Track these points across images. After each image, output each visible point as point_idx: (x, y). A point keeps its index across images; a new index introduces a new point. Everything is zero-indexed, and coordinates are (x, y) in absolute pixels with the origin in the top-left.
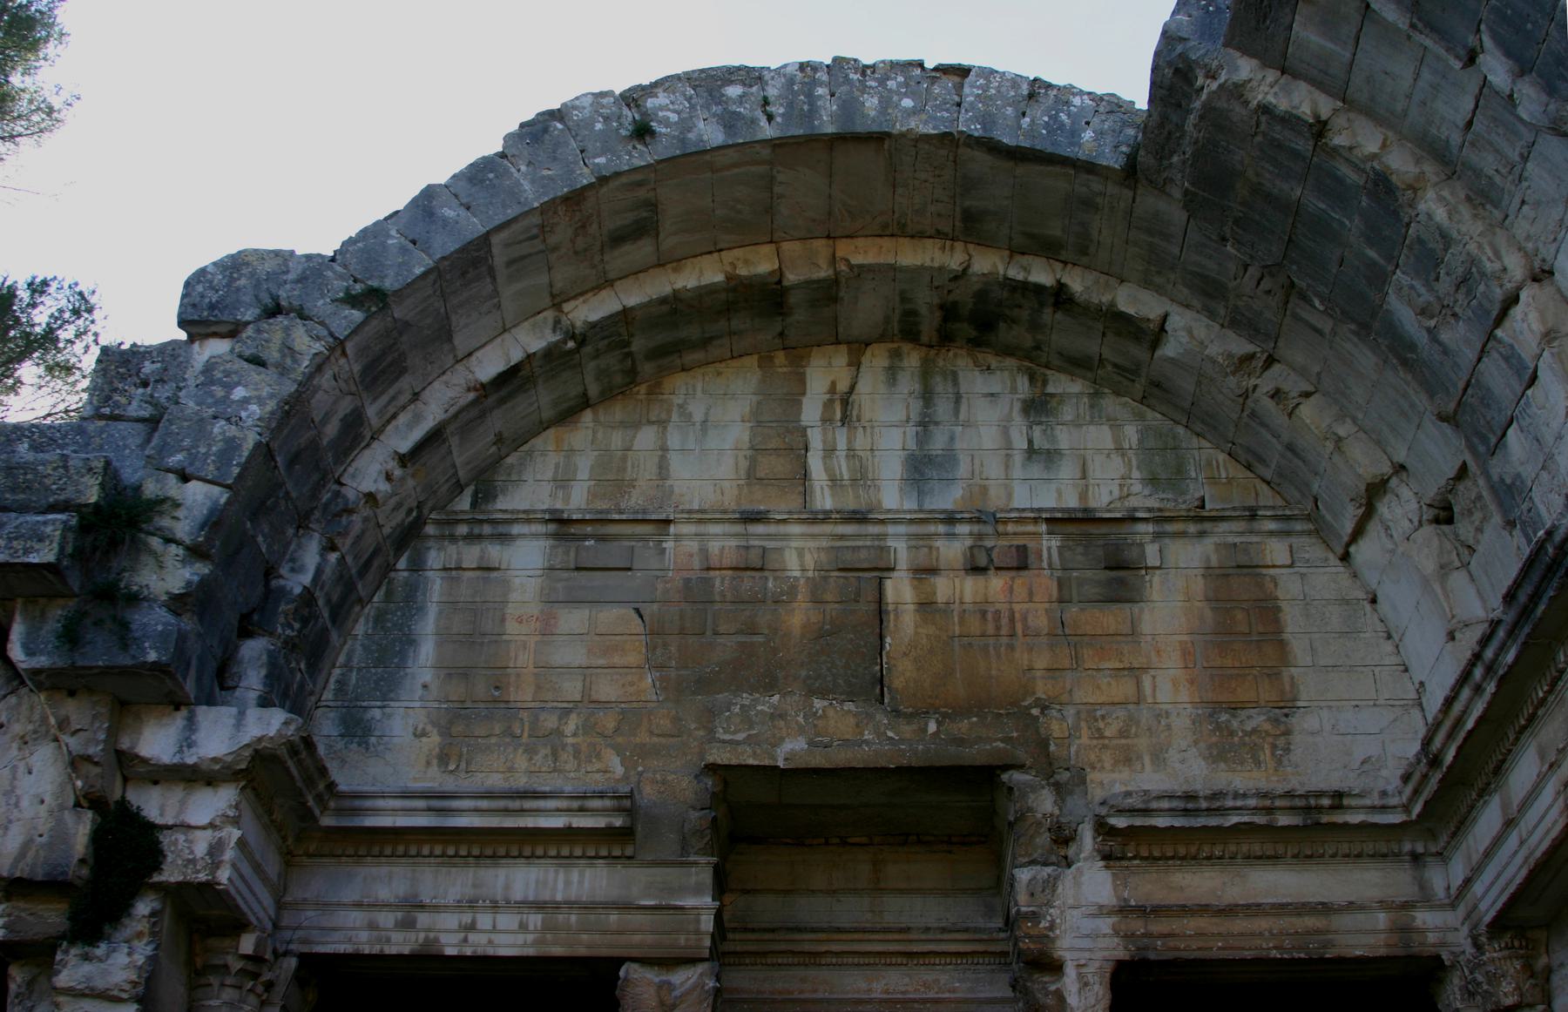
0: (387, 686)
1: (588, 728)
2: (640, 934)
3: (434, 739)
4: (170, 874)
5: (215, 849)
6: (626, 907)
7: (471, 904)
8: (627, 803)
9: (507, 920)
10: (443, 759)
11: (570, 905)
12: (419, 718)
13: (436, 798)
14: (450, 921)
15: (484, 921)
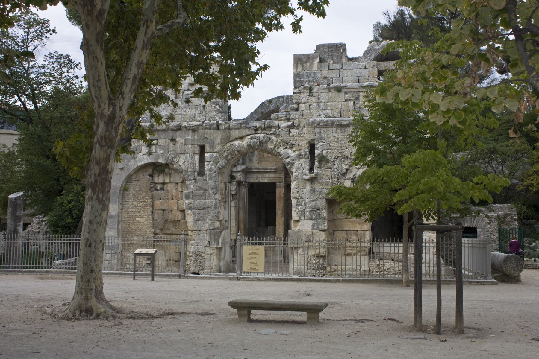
0: (253, 156)
1: (272, 159)
2: (278, 180)
3: (258, 161)
4: (236, 180)
5: (240, 178)
6: (276, 177)
7: (262, 177)
8: (276, 169)
9: (266, 179)
10: (259, 163)
11: (271, 177)
12: (256, 159)
13: (259, 169)
14: (261, 179)
15: (264, 179)
